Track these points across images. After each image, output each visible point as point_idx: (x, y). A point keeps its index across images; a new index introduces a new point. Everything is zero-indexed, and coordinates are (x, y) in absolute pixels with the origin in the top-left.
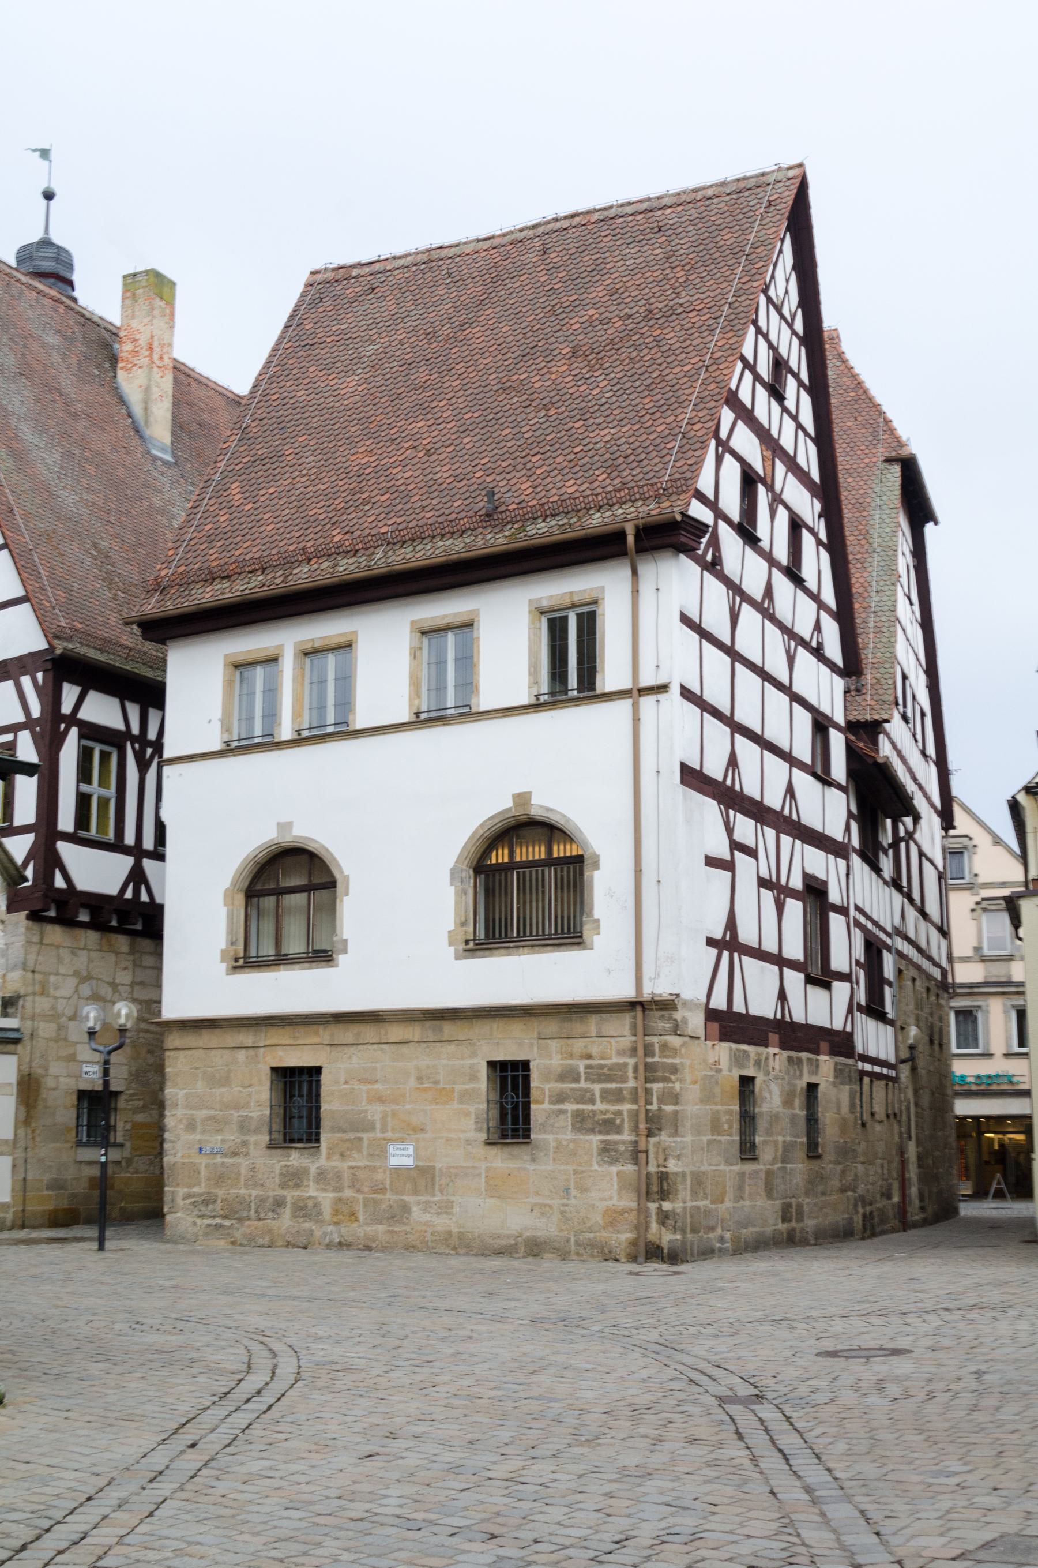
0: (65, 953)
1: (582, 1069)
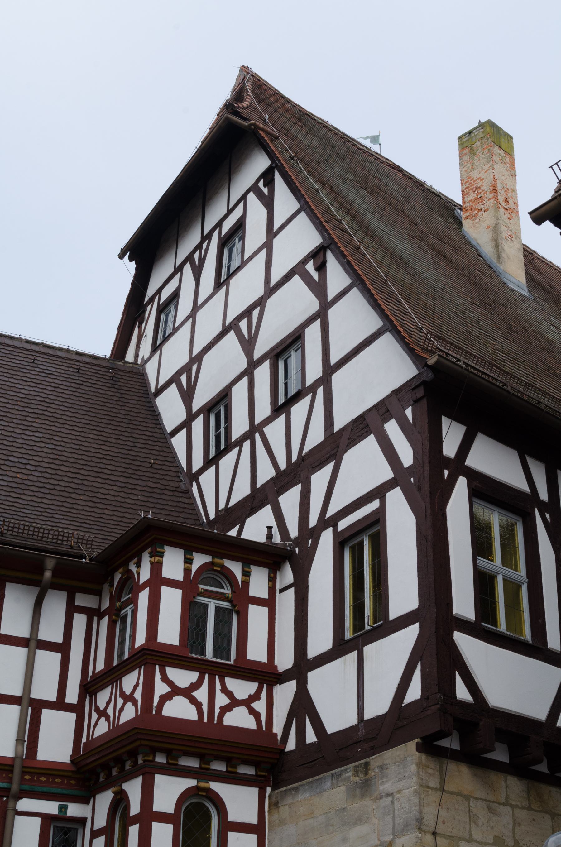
0: (478, 808)
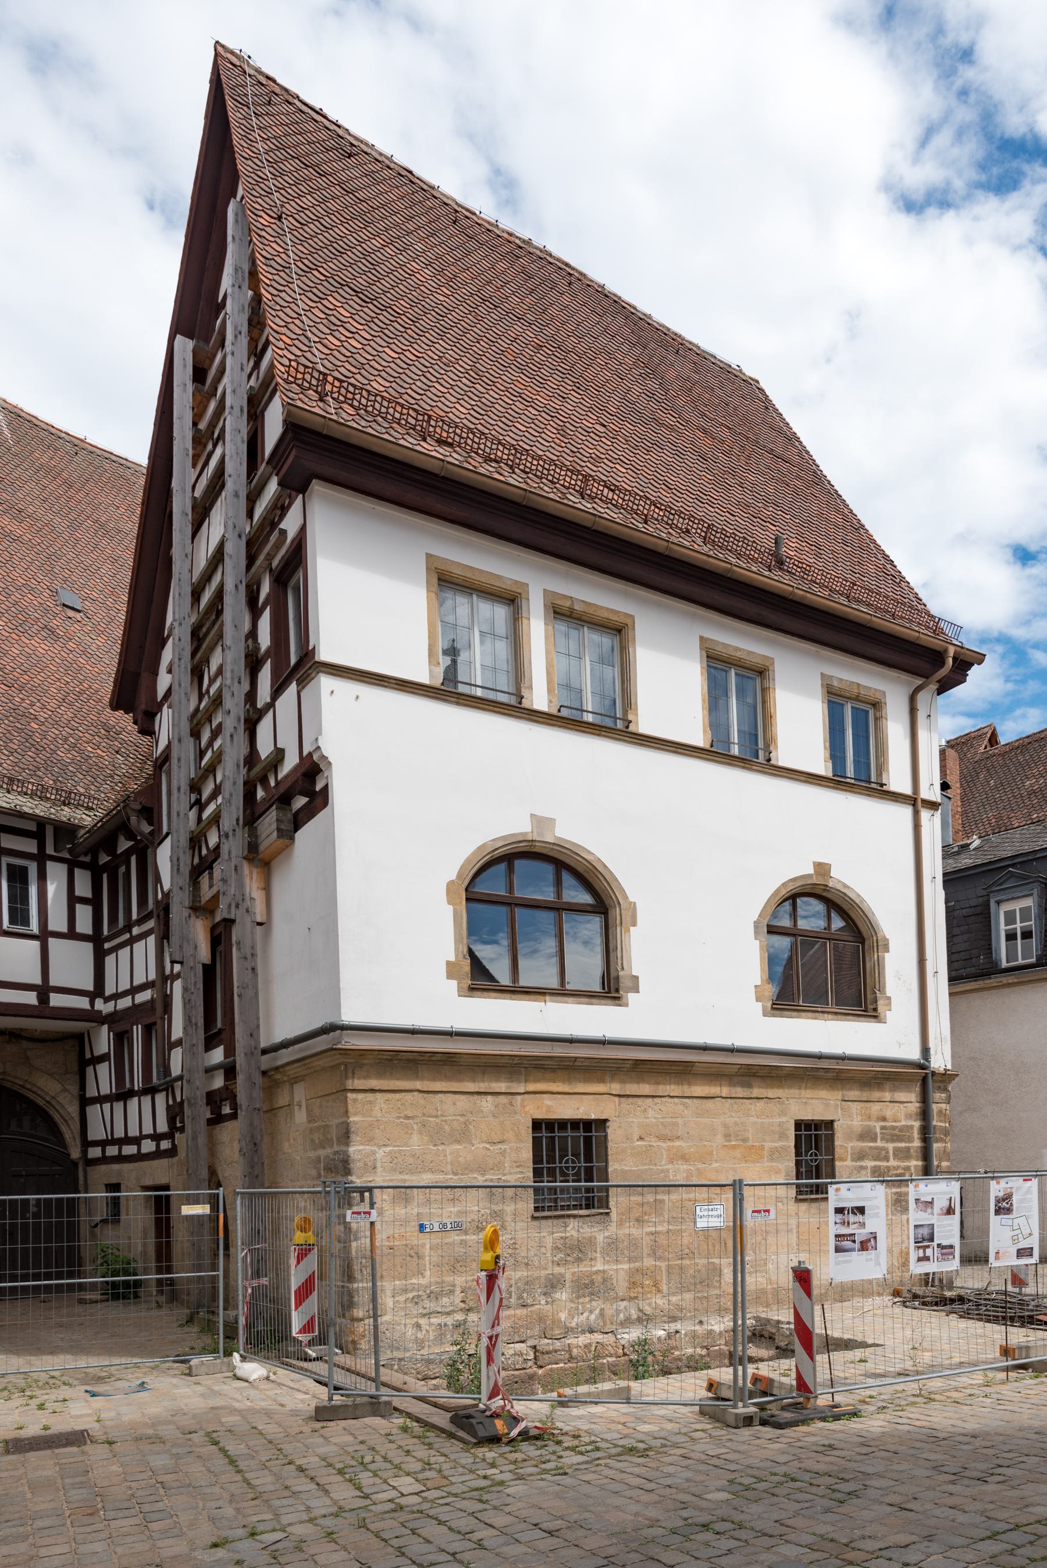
1: (878, 1130)
